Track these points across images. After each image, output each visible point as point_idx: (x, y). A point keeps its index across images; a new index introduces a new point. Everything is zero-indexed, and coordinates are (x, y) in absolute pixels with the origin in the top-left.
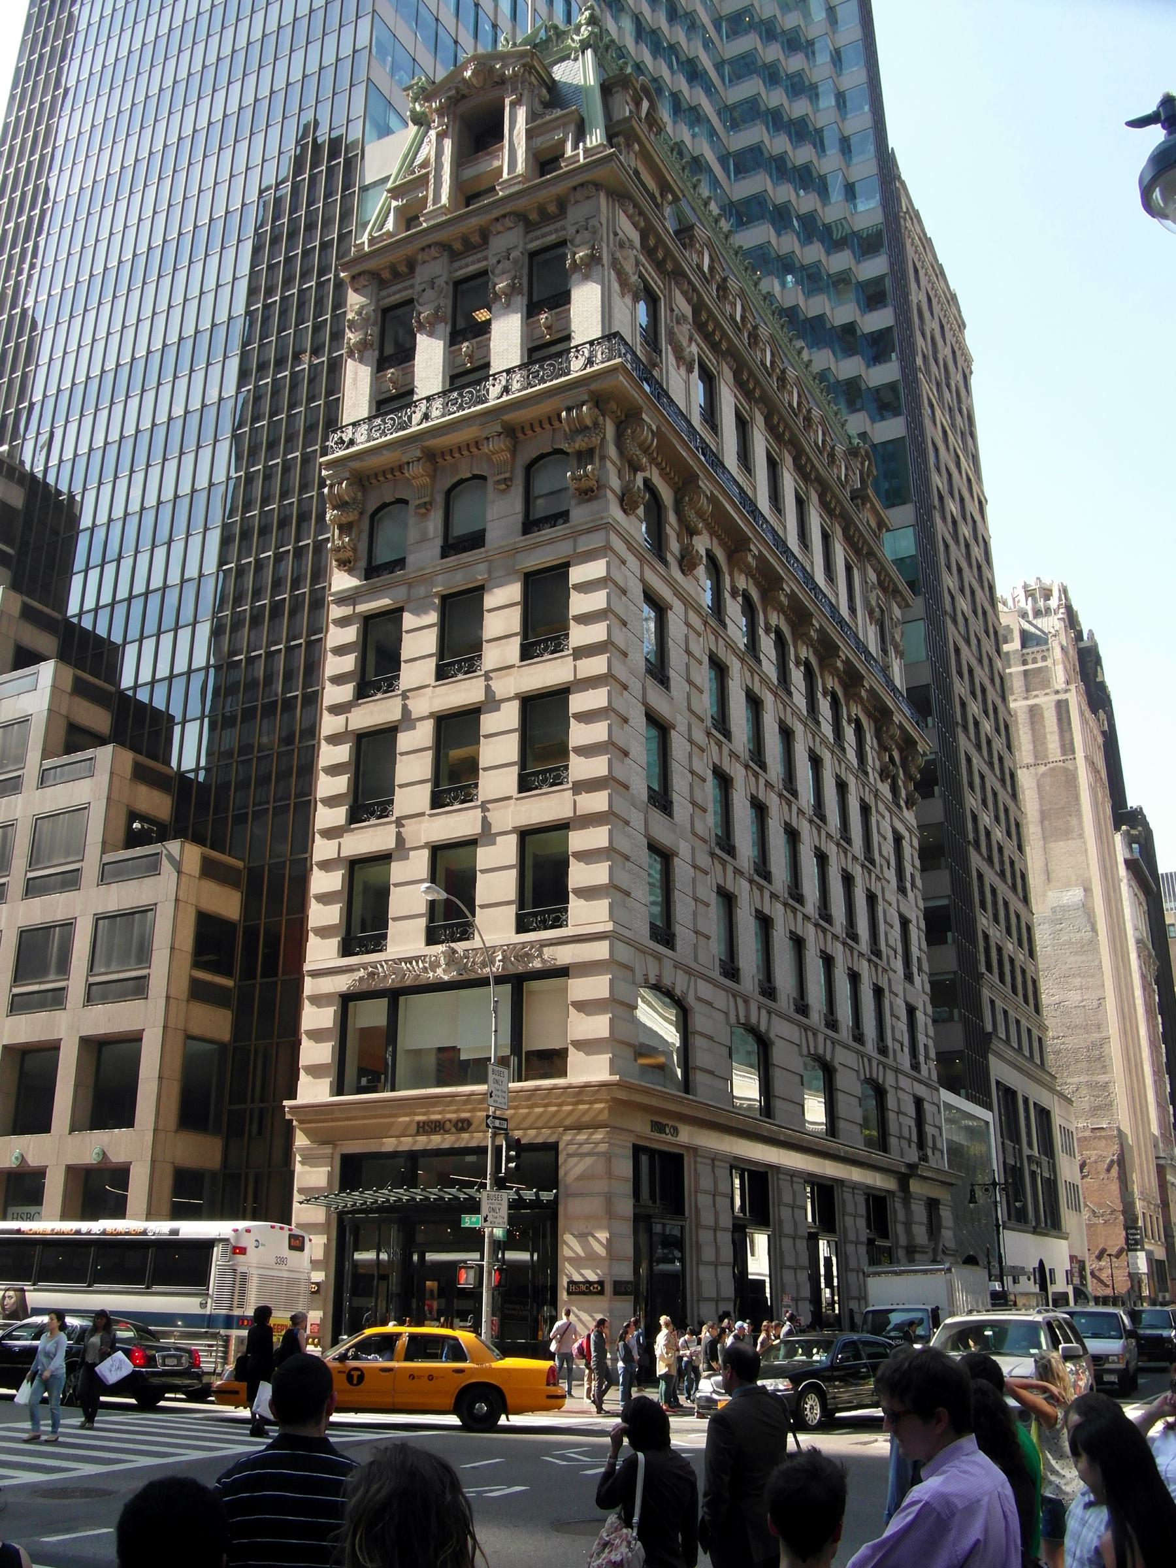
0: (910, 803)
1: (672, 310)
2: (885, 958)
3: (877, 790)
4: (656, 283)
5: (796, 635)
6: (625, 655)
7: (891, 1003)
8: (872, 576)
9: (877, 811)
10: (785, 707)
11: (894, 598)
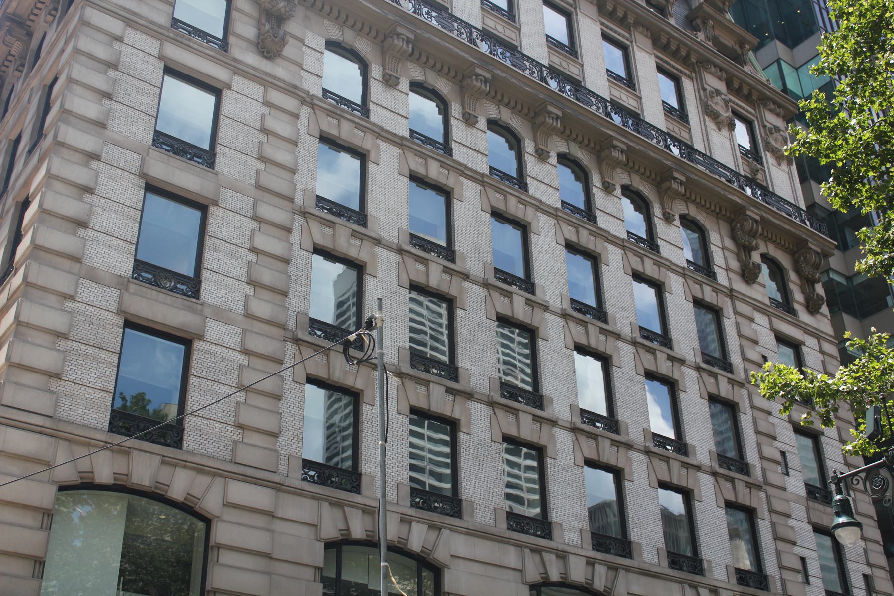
0: (812, 307)
2: (757, 473)
3: (731, 290)
5: (536, 127)
6: (102, 125)
7: (773, 525)
8: (713, 82)
9: (736, 313)
10: (504, 196)
11: (765, 106)
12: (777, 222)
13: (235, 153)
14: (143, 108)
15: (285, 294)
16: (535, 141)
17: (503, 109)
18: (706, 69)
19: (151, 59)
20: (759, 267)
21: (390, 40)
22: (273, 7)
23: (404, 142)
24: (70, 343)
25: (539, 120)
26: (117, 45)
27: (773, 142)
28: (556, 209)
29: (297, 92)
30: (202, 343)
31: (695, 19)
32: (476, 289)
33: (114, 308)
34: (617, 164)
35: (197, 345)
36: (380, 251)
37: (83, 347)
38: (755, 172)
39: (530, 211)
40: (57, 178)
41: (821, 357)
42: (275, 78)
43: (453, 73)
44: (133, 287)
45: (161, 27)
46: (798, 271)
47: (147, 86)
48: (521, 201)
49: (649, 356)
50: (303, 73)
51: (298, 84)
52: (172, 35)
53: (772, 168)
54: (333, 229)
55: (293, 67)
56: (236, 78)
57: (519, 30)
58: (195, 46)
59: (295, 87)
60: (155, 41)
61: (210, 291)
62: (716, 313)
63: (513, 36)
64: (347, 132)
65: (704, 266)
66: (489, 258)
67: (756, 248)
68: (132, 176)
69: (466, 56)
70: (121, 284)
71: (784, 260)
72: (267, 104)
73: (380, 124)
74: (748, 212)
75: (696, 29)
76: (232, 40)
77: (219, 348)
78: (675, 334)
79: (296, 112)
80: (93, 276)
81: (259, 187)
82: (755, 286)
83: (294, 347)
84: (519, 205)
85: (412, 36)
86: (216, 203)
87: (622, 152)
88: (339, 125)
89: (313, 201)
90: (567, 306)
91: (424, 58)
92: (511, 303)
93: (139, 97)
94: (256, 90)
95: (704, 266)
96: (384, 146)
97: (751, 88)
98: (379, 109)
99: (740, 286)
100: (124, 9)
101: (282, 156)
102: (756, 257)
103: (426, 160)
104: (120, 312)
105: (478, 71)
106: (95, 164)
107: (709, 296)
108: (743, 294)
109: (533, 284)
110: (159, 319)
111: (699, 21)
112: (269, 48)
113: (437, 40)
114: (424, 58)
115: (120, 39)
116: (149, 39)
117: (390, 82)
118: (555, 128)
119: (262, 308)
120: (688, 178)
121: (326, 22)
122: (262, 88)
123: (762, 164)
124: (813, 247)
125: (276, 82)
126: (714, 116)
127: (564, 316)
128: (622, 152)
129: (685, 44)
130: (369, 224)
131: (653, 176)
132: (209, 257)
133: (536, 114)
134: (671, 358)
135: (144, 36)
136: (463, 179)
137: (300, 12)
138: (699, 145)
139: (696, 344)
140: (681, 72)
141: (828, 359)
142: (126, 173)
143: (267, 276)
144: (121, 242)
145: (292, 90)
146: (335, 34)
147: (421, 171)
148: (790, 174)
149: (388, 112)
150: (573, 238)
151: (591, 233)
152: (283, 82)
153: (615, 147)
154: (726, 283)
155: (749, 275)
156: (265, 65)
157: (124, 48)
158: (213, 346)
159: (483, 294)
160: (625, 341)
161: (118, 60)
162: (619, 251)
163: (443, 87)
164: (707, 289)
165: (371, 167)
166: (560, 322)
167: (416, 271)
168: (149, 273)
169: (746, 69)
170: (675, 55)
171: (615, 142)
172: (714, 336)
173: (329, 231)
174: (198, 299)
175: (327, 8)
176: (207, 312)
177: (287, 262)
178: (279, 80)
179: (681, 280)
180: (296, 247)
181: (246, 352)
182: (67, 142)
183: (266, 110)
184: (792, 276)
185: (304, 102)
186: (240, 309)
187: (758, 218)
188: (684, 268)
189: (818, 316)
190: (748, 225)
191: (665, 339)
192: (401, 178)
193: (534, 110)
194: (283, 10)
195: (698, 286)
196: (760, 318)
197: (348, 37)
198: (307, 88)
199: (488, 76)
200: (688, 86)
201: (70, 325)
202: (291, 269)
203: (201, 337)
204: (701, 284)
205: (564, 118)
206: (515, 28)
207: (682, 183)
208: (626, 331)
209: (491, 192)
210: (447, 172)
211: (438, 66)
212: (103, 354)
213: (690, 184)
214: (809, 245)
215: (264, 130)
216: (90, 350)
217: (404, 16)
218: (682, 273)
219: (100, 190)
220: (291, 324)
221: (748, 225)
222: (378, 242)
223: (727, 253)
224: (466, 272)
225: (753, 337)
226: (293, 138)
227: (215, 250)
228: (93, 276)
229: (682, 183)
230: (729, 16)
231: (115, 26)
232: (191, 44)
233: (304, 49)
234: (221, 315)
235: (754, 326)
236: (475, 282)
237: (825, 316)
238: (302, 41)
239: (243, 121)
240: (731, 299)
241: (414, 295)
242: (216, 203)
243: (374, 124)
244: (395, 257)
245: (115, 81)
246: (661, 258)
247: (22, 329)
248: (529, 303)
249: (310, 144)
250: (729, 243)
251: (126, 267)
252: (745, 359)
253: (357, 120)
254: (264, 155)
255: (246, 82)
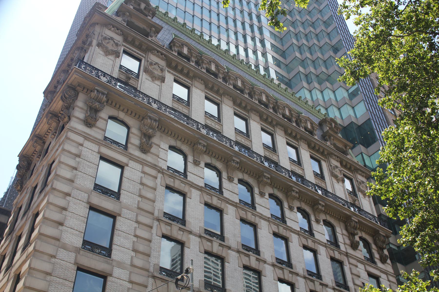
0: (383, 260)
1: (148, 61)
3: (347, 253)
4: (138, 53)
5: (260, 183)
6: (72, 181)
8: (335, 163)
9: (349, 263)
10: (246, 212)
11: (357, 172)
12: (365, 222)
13: (128, 193)
14: (90, 174)
15: (149, 256)
16: (259, 188)
17: (245, 175)
18: (331, 157)
19: (95, 153)
20: (358, 242)
21: (196, 146)
22: (147, 132)
23: (202, 189)
24: (52, 277)
25: (260, 179)
26: (80, 147)
27: (362, 188)
28: (269, 218)
29: (156, 167)
30: (111, 278)
31: (325, 136)
32: (234, 253)
33: (73, 262)
34: (294, 198)
35: (109, 279)
36: (191, 237)
37: (58, 279)
38: (355, 201)
39: (257, 218)
40: (51, 204)
41: (388, 283)
42: (147, 161)
43: (223, 159)
44: (82, 252)
45: (99, 140)
46: (376, 244)
47: (92, 165)
48: (253, 214)
49: (312, 283)
50: (159, 159)
51: (157, 164)
52: (104, 143)
53: (362, 199)
54: (171, 227)
55: (154, 157)
56: (130, 161)
57: (251, 141)
58: (114, 148)
59: (156, 165)
60: (96, 146)
61: (116, 254)
62: (341, 263)
63: (249, 144)
64: (177, 185)
65: (334, 243)
66: (239, 240)
67: (357, 234)
68: (84, 203)
69: (229, 152)
70: (77, 251)
71: (369, 239)
72: (143, 172)
73: (192, 181)
74: (353, 218)
75: (326, 140)
76: (129, 145)
77: (119, 280)
78: (323, 273)
79: (156, 176)
80: (65, 247)
81: (139, 208)
82: (357, 251)
83: (153, 280)
84: (252, 216)
85: (206, 144)
86: (120, 215)
87: (297, 192)
88: (174, 181)
89: (163, 214)
90: (274, 261)
91: (211, 153)
92: (250, 260)
93: (89, 169)
94: (139, 167)
95: (334, 243)
96: (193, 190)
97: (351, 165)
98: (191, 175)
99: (350, 251)
100: (85, 132)
101: (149, 195)
102: (357, 238)
103: (211, 197)
104: (76, 263)
105: (234, 158)
106: (68, 198)
107: (337, 256)
108: (352, 255)
109: (259, 251)
110: (93, 267)
111: (327, 137)
112: (145, 148)
113: (217, 146)
114: (211, 153)
115: (82, 145)
116: (94, 145)
117: (196, 163)
118: (296, 197)
119: (139, 262)
120: (325, 204)
121: (169, 138)
122: (141, 166)
123: (357, 197)
124: (382, 233)
125: (147, 163)
126: (336, 177)
127: (273, 265)
128: (297, 192)
129: (322, 147)
130: (187, 225)
131: (310, 203)
132: (116, 239)
133: (259, 177)
134: (322, 284)
135: (92, 144)
136: (228, 205)
137: (158, 134)
138: (330, 190)
139: (333, 278)
140: (321, 158)
141: (392, 284)
142: (81, 202)
143: (141, 247)
144: (77, 232)
145: (154, 167)
146: (173, 143)
147: (209, 201)
148: (370, 201)
149: (195, 176)
150: (276, 231)
151: (284, 228)
152: (151, 163)
153: (294, 191)
154: (344, 250)
155: (354, 246)
156: (143, 156)
157: (83, 148)
158: (116, 279)
159: (237, 256)
160: (301, 276)
161: (81, 154)
162: (297, 236)
163: (219, 165)
164: (336, 253)
165: (188, 200)
166: (271, 268)
167: (207, 246)
168: (89, 246)
169: (348, 157)
170: (318, 151)
171: (294, 189)
172: (340, 274)
173: (169, 228)
174: (110, 258)
175: (170, 133)
176: (114, 264)
177: (150, 241)
178: (149, 162)
179: (324, 249)
180: (154, 235)
181: (131, 282)
182: (57, 188)
183: (143, 175)
184: (374, 246)
185: (159, 172)
186: (129, 262)
187: (357, 221)
188: (325, 244)
189: (386, 264)
190: (353, 224)
191: (319, 276)
192: (201, 204)
193: (258, 175)
194: (151, 133)
195: (332, 251)
196: (360, 266)
197: (179, 144)
198: (160, 166)
199: (238, 160)
200: (324, 164)
201: (53, 269)
202: (152, 244)
203: (111, 275)
204: (333, 250)
205: (271, 179)
206: (250, 140)
207: (323, 206)
208: (301, 272)
209: (240, 210)
210: (221, 202)
211: (217, 156)
212: (67, 283)
213: (326, 206)
214: (380, 232)
215: (142, 184)
216: (61, 281)
217: (202, 135)
218: (325, 246)
219: (70, 209)
220: (151, 269)
221: (353, 224)
222: (190, 232)
223: (344, 237)
224: (229, 246)
225: (358, 274)
226: (154, 187)
227: (119, 236)
228: (65, 247)
229: (323, 206)
230: (340, 135)
231: (80, 139)
232: (112, 147)
233: (160, 149)
234: (120, 265)
235: (358, 269)
236: (233, 250)
237: (389, 264)
238: (159, 146)
239: (133, 179)
240: (347, 257)
241: (206, 256)
242: (120, 215)
243: (189, 181)
244: (198, 239)
245: (79, 162)
246: (315, 239)
247: (31, 271)
248: (257, 259)
249: (161, 189)
250: (345, 232)
251: (79, 243)
252: (354, 284)
253: (182, 179)
254: (141, 194)
255: (135, 163)
